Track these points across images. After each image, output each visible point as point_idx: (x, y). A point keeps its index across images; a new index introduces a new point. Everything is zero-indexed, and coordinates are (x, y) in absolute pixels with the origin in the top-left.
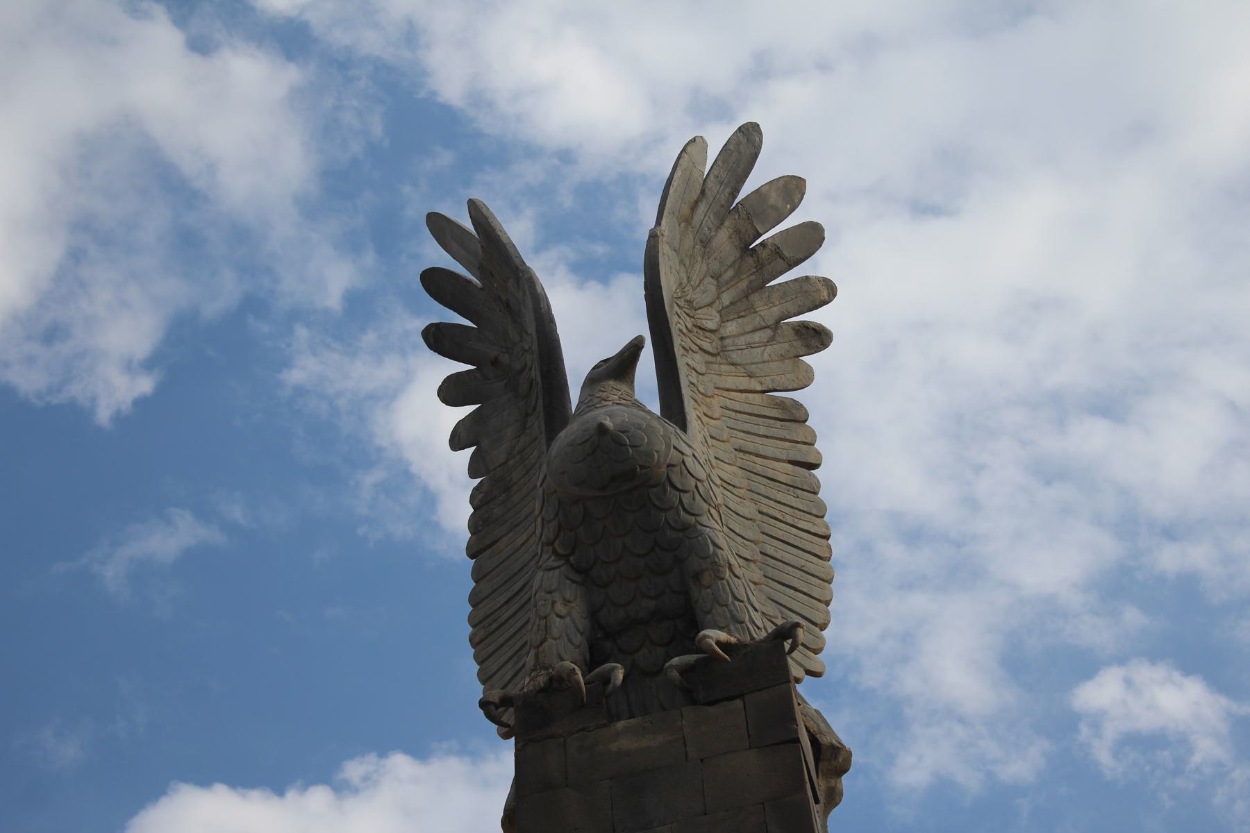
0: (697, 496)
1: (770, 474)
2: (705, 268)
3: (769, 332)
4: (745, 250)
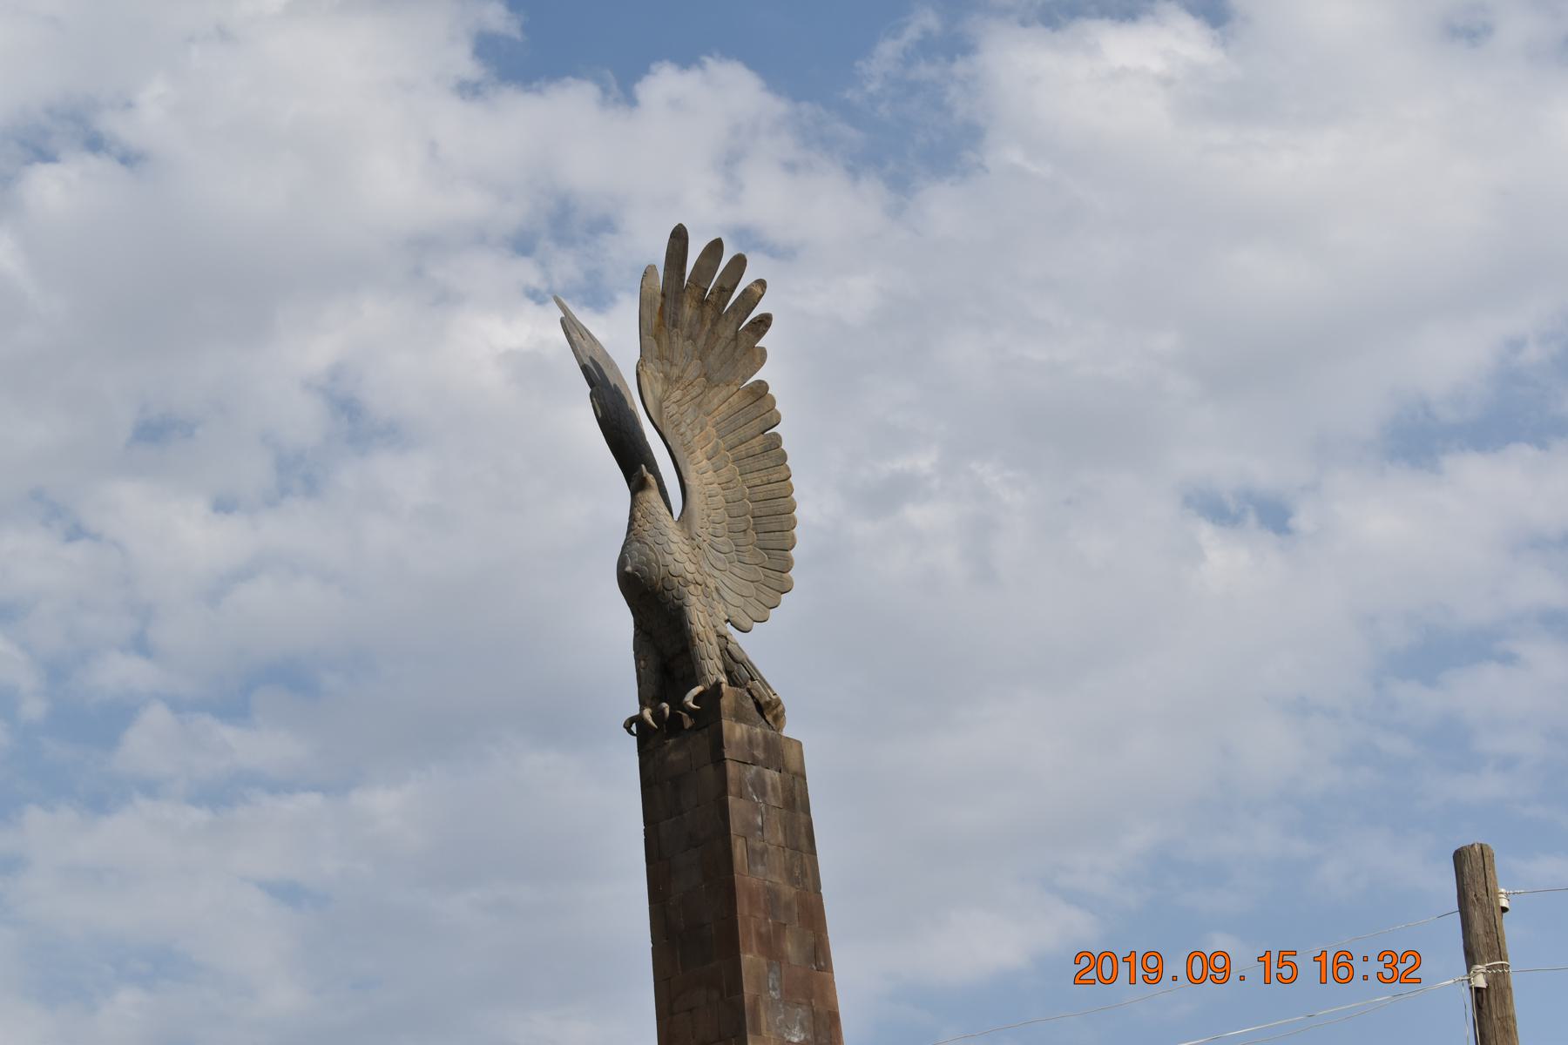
4: (702, 302)
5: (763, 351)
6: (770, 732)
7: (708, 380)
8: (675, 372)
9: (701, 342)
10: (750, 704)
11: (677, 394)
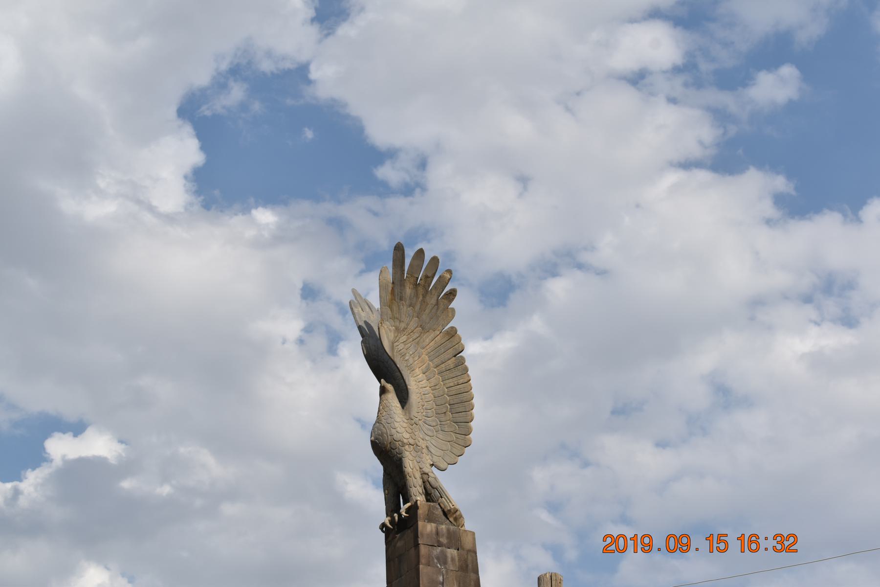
4: (416, 285)
5: (453, 310)
6: (452, 527)
7: (423, 329)
8: (403, 325)
10: (439, 512)
11: (404, 338)
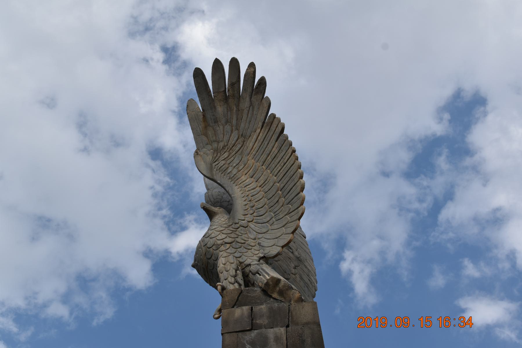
0: (215, 251)
1: (273, 156)
2: (221, 127)
3: (251, 107)
4: (226, 99)
6: (276, 305)
8: (221, 145)
9: (234, 122)
11: (226, 155)
